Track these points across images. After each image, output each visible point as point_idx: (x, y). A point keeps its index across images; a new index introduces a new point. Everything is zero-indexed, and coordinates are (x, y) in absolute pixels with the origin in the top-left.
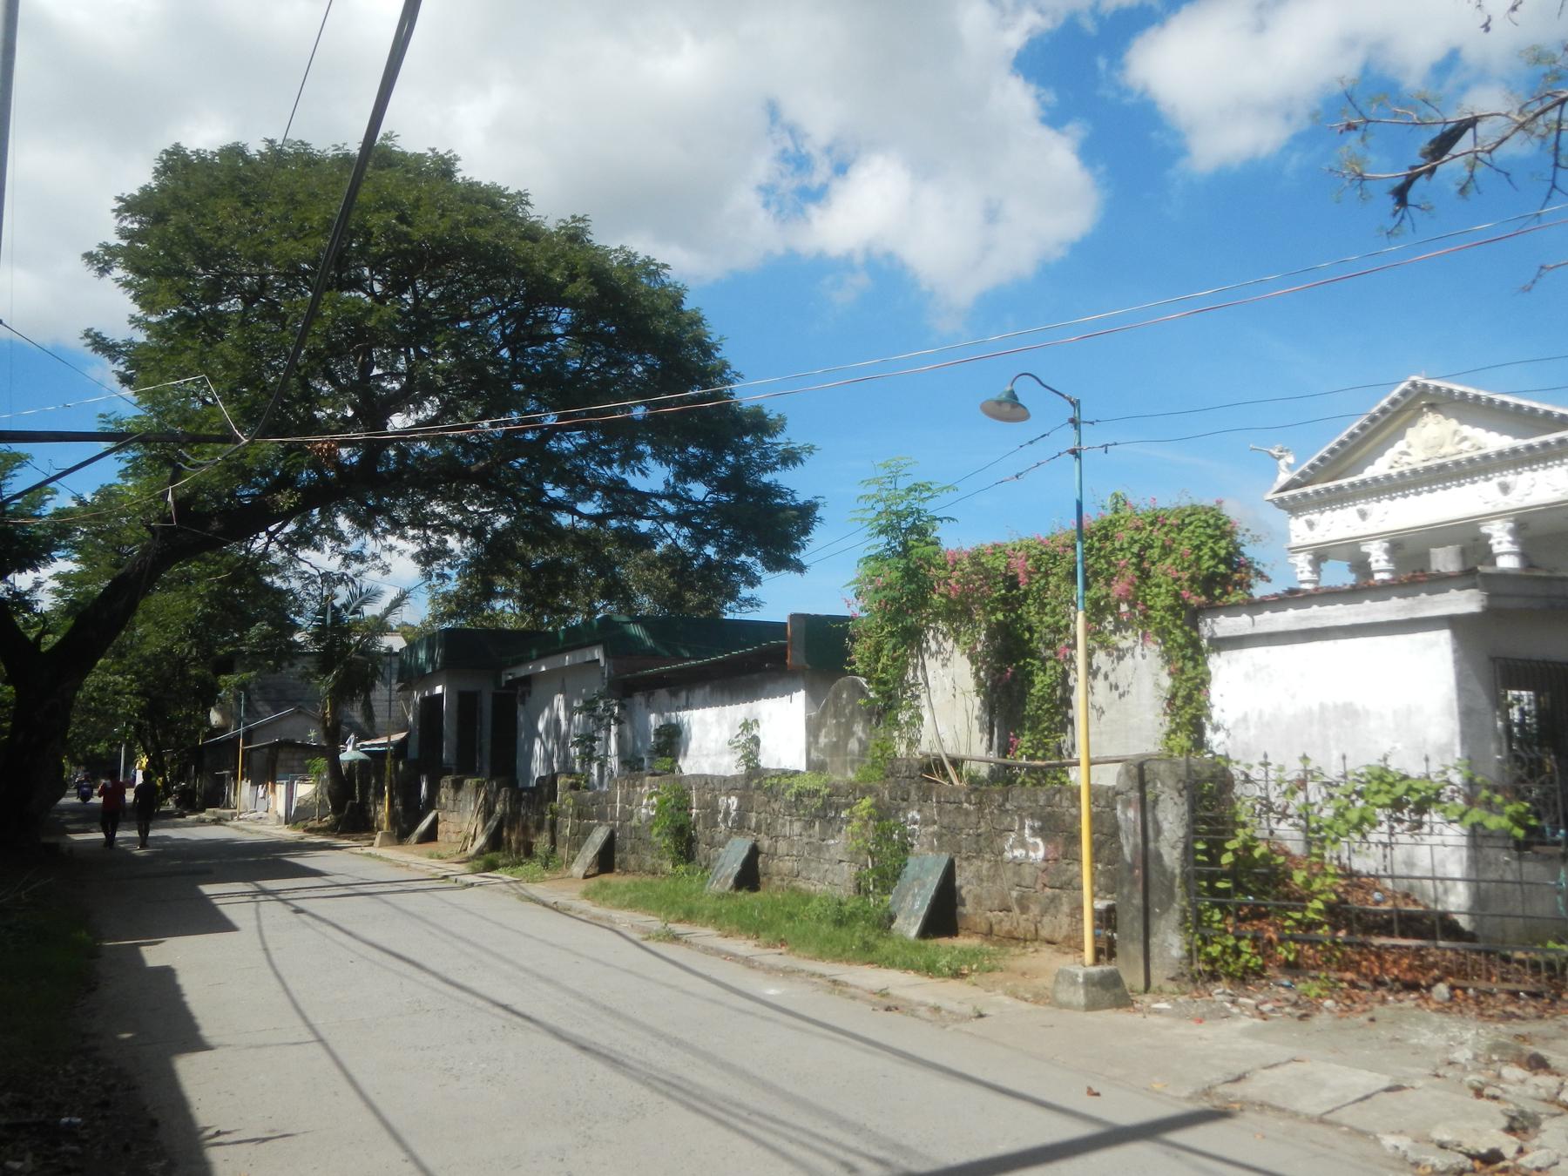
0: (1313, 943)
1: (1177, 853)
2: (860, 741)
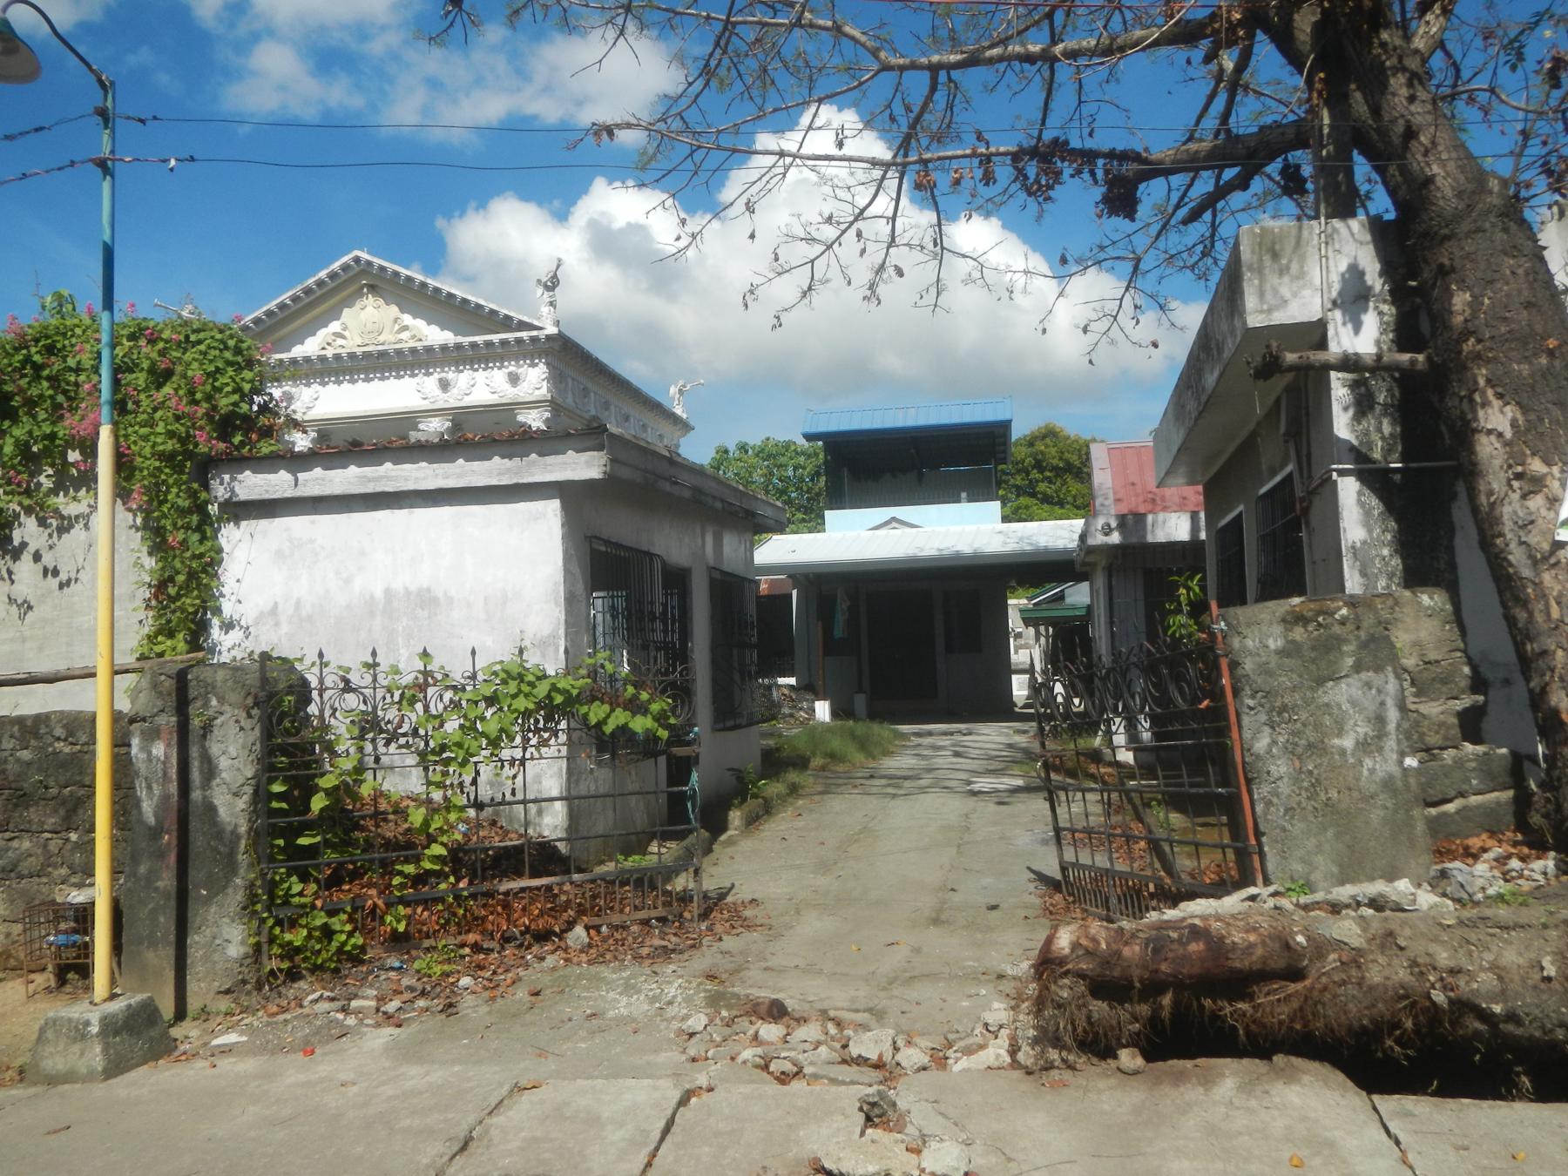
0: (427, 903)
1: (242, 803)
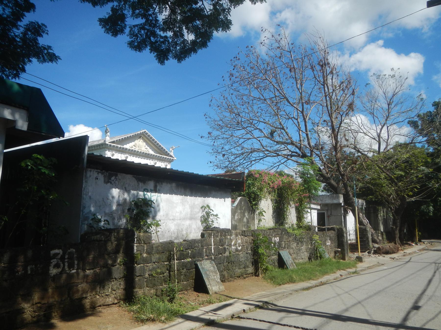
2: (247, 218)
